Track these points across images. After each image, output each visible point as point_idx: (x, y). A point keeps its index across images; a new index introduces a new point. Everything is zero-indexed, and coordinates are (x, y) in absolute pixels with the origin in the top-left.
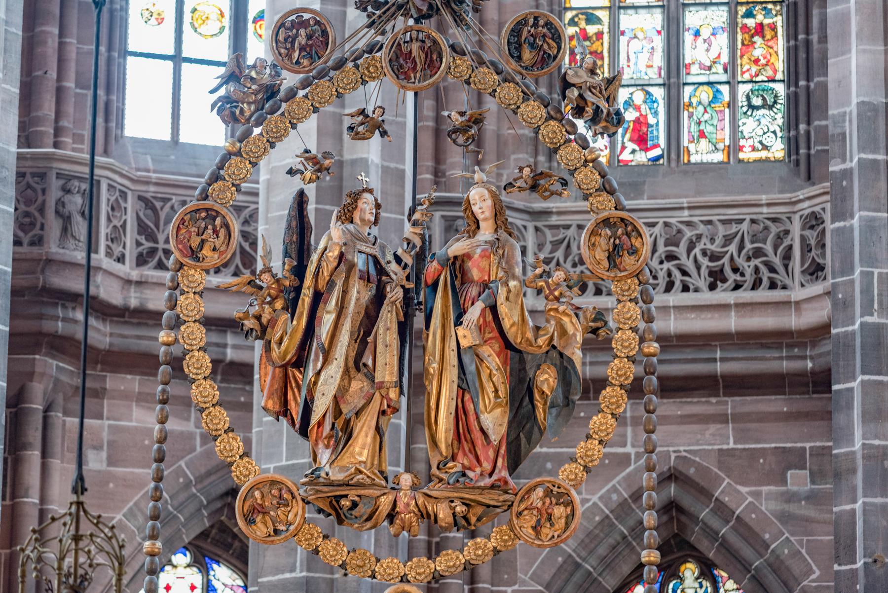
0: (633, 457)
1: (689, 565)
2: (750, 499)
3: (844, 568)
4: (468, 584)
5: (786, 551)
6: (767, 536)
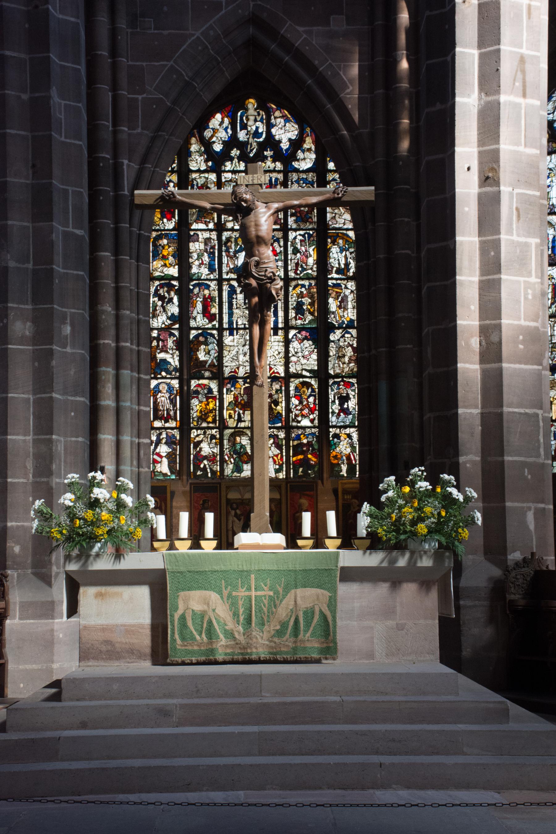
0: (224, 4)
1: (252, 100)
2: (305, 36)
3: (435, 12)
4: (111, 92)
5: (329, 73)
6: (316, 62)
